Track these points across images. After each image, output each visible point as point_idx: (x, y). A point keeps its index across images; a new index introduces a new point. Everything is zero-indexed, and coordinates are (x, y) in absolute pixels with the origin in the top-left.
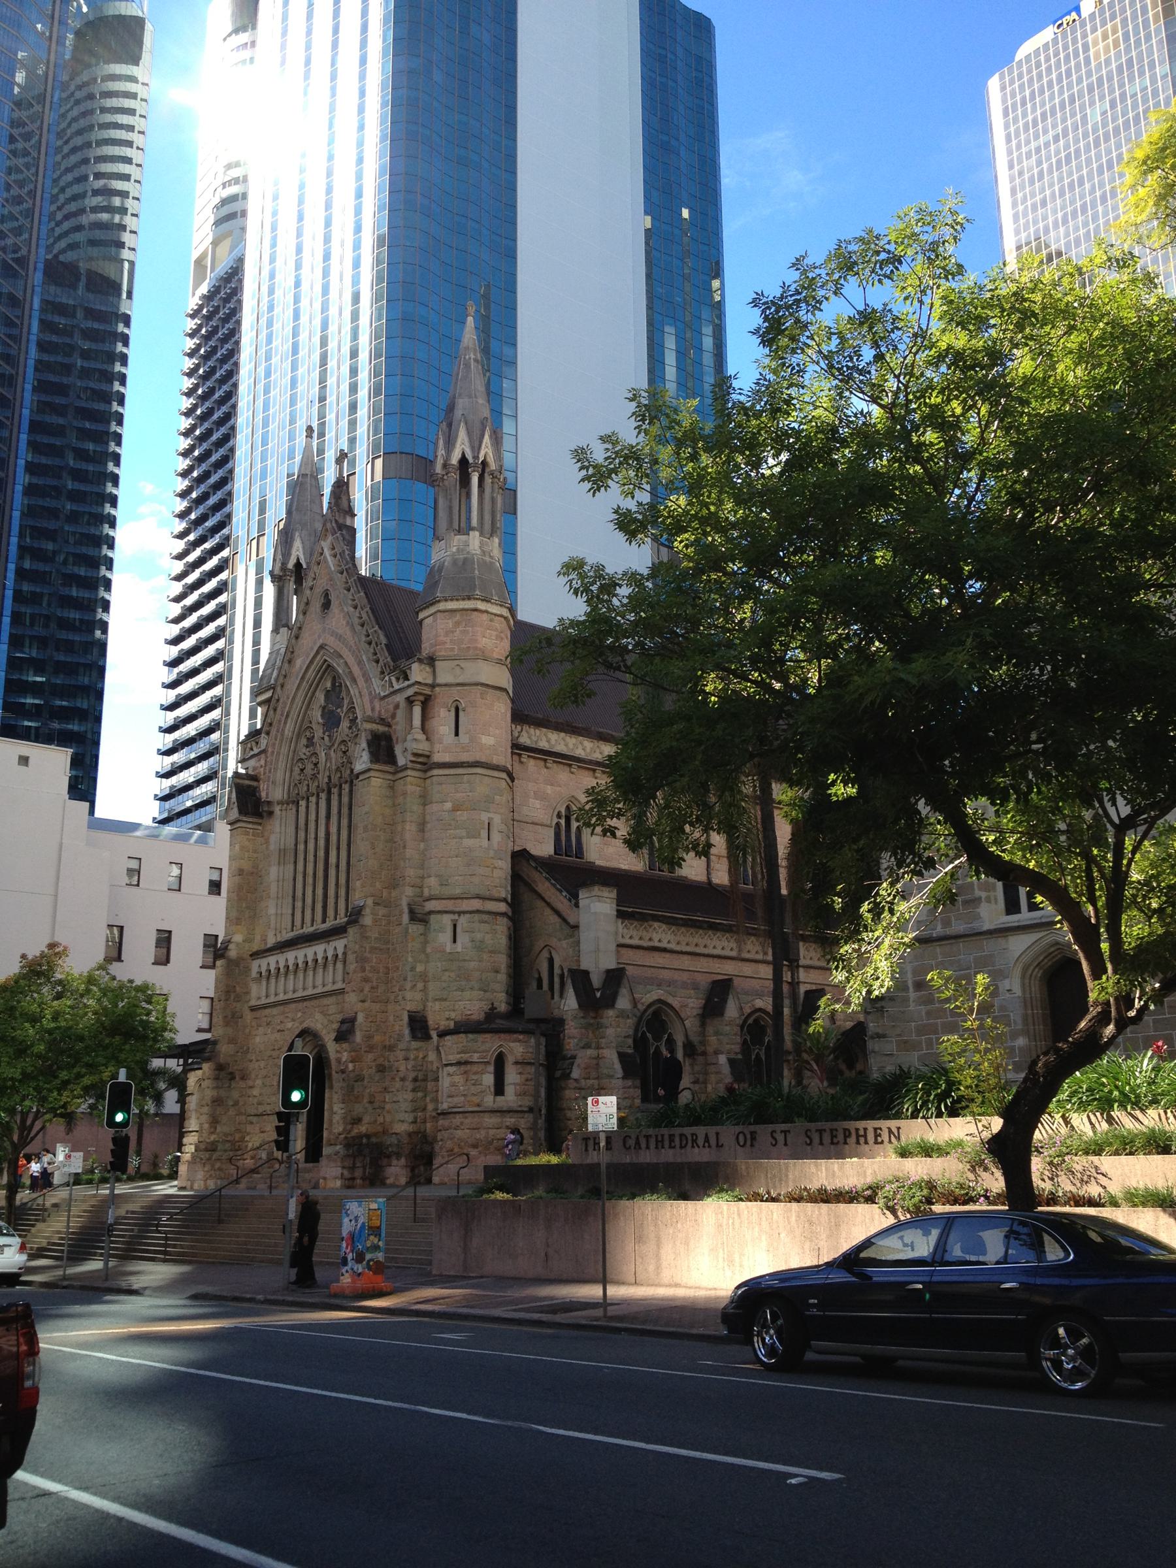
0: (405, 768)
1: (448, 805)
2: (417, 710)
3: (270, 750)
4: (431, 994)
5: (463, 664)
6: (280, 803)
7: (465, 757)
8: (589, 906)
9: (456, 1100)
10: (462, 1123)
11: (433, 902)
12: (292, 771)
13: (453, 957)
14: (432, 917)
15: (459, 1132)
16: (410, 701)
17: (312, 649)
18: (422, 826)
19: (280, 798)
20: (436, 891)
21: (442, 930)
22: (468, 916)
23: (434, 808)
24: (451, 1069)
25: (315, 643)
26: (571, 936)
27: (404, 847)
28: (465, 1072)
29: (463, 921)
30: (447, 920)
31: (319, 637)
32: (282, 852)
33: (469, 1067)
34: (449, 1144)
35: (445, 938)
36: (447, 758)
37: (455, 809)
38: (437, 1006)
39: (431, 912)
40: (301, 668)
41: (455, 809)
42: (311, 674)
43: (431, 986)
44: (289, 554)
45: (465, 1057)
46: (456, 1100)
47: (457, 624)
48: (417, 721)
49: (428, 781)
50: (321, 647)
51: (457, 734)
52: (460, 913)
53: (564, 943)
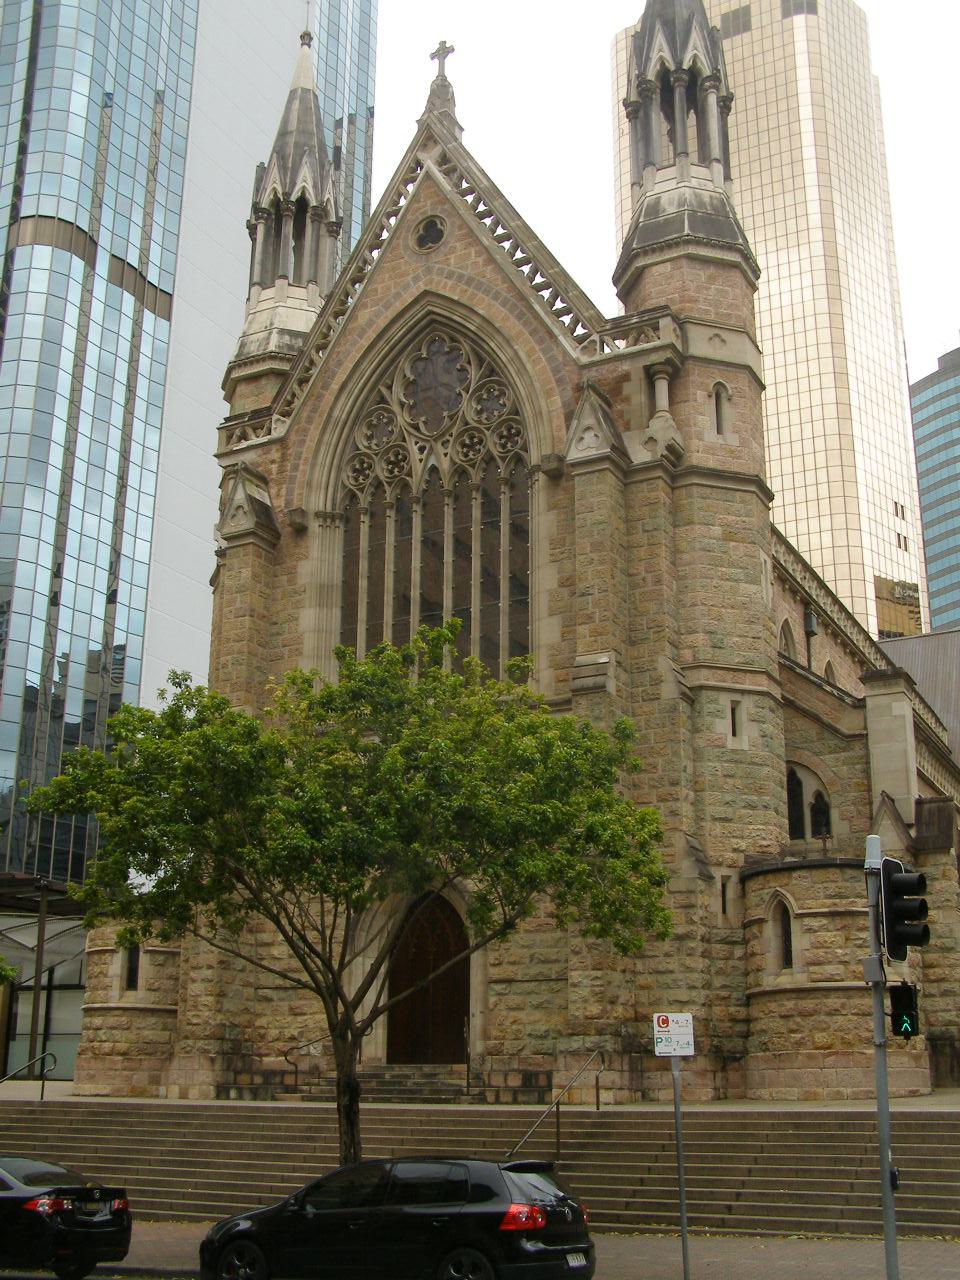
0: (647, 467)
1: (717, 530)
2: (662, 387)
3: (293, 437)
4: (710, 810)
5: (724, 335)
6: (317, 515)
7: (734, 466)
8: (889, 707)
9: (830, 969)
10: (843, 1006)
11: (705, 672)
12: (339, 469)
13: (737, 756)
14: (705, 694)
15: (840, 1018)
16: (650, 375)
17: (398, 295)
18: (676, 551)
19: (321, 508)
20: (706, 654)
21: (717, 714)
22: (757, 697)
23: (699, 529)
24: (814, 923)
25: (406, 287)
26: (844, 750)
27: (658, 582)
28: (843, 928)
29: (747, 705)
30: (725, 701)
31: (416, 279)
32: (323, 590)
33: (848, 921)
34: (820, 1038)
35: (723, 726)
36: (711, 463)
37: (728, 537)
38: (718, 828)
39: (702, 688)
40: (370, 323)
41: (728, 537)
42: (398, 332)
43: (708, 796)
44: (293, 184)
45: (842, 905)
46: (830, 969)
47: (712, 279)
48: (662, 399)
49: (677, 492)
50: (426, 293)
51: (719, 431)
52: (743, 692)
53: (828, 758)
